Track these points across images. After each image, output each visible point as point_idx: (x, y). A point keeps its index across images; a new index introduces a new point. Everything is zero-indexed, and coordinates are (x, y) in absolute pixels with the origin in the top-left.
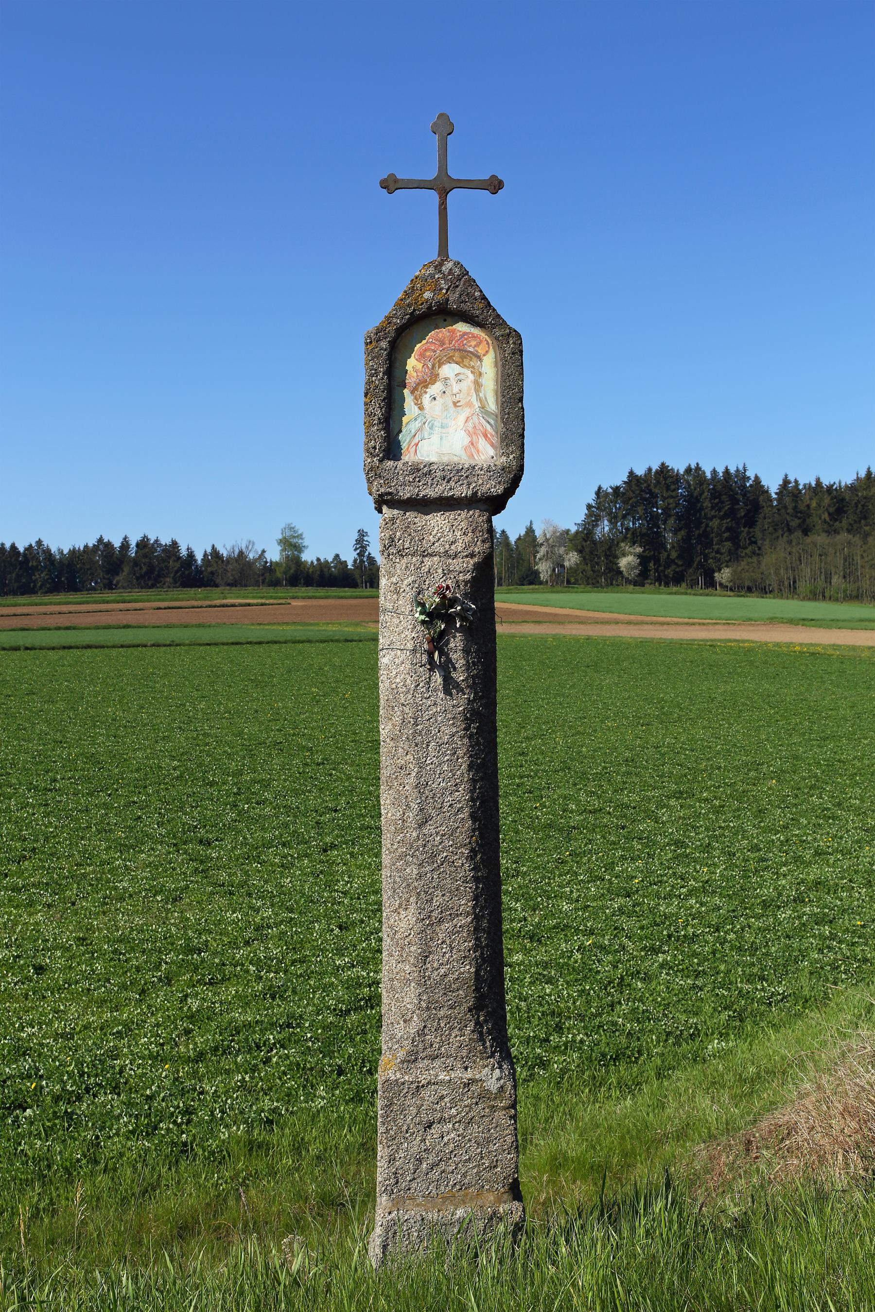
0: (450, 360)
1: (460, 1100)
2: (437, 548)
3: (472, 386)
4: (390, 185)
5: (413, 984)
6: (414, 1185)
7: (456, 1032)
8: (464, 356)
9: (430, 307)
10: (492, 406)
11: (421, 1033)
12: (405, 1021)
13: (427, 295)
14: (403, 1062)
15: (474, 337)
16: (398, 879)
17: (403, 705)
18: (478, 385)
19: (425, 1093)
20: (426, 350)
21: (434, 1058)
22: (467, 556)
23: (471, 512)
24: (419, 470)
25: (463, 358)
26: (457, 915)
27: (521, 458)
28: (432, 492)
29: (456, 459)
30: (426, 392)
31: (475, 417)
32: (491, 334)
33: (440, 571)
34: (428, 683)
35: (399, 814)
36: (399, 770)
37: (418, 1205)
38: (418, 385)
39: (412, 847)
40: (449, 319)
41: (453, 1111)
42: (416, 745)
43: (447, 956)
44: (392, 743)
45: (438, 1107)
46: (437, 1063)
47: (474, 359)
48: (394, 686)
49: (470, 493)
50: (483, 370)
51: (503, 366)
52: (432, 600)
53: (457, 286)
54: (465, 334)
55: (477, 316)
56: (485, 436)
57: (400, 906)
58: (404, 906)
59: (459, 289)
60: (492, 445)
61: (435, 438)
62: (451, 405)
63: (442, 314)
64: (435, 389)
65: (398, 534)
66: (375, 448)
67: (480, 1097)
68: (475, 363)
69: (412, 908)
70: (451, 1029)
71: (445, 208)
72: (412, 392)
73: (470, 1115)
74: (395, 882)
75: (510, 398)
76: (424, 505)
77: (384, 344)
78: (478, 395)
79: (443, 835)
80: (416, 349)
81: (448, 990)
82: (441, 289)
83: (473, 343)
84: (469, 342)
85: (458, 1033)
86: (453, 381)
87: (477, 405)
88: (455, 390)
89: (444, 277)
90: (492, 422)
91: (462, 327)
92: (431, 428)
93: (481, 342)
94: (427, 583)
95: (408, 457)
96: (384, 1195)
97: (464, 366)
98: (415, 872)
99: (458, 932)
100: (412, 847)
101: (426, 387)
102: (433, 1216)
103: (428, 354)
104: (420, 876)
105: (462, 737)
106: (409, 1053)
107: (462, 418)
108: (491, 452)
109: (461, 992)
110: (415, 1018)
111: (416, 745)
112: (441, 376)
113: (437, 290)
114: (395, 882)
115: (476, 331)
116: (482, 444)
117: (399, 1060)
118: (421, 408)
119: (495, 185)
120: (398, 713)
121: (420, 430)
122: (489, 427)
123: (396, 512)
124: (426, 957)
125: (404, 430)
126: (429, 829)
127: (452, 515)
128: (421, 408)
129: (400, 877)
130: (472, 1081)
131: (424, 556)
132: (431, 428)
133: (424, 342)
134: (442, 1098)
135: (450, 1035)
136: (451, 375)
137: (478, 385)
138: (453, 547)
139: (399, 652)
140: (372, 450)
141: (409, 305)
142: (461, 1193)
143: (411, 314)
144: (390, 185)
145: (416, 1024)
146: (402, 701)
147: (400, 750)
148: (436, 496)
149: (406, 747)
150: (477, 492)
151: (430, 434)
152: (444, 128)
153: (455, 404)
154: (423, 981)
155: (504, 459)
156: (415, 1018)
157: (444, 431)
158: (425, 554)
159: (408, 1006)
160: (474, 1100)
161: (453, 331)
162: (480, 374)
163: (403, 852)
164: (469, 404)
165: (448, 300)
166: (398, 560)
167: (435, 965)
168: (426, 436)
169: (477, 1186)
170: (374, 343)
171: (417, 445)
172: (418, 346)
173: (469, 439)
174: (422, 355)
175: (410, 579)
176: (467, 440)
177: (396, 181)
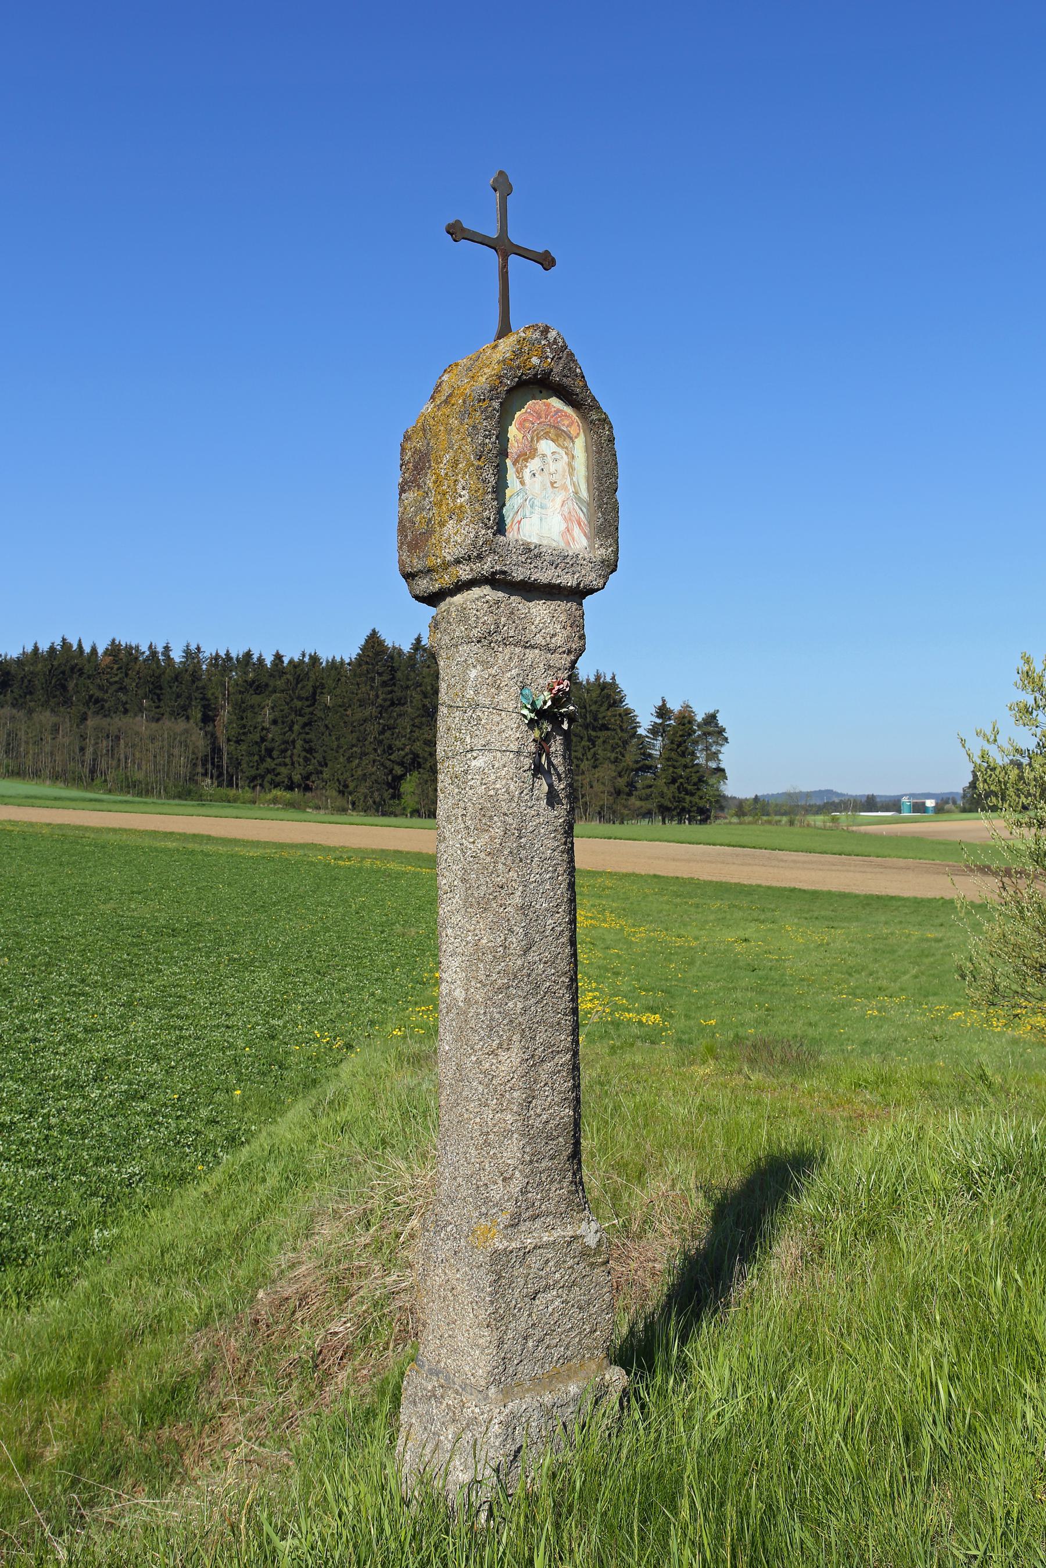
0: (546, 436)
1: (564, 1262)
2: (539, 639)
3: (567, 468)
4: (456, 232)
5: (515, 1136)
6: (520, 1368)
7: (556, 1185)
8: (560, 435)
9: (536, 375)
10: (584, 494)
11: (524, 1192)
12: (504, 1180)
13: (535, 360)
14: (506, 1227)
15: (567, 416)
16: (497, 1016)
17: (505, 814)
18: (571, 467)
19: (531, 1259)
20: (525, 420)
21: (534, 1218)
22: (564, 652)
23: (569, 604)
24: (530, 550)
25: (558, 436)
26: (558, 1052)
27: (616, 552)
28: (544, 576)
29: (554, 544)
30: (526, 467)
31: (570, 502)
32: (584, 417)
33: (541, 665)
34: (532, 790)
35: (499, 940)
36: (498, 889)
37: (528, 1390)
38: (519, 456)
39: (516, 977)
40: (544, 392)
41: (557, 1275)
42: (521, 861)
43: (549, 1099)
44: (488, 859)
45: (543, 1273)
46: (538, 1224)
47: (568, 440)
48: (492, 793)
49: (575, 583)
50: (575, 453)
51: (599, 452)
52: (544, 699)
53: (560, 358)
54: (558, 411)
55: (577, 395)
56: (580, 525)
57: (500, 1046)
58: (505, 1046)
59: (562, 361)
60: (585, 535)
61: (535, 518)
62: (549, 484)
63: (540, 384)
64: (534, 464)
65: (503, 619)
66: (489, 519)
67: (583, 1254)
68: (567, 443)
69: (516, 1047)
70: (552, 1182)
71: (507, 272)
72: (514, 464)
73: (573, 1276)
74: (492, 1019)
75: (608, 487)
76: (530, 590)
77: (496, 404)
78: (572, 479)
79: (546, 963)
80: (516, 416)
81: (550, 1138)
82: (547, 357)
83: (566, 422)
84: (562, 420)
85: (558, 1186)
86: (549, 459)
87: (571, 489)
88: (552, 470)
89: (549, 345)
90: (585, 510)
91: (555, 403)
92: (532, 507)
93: (572, 423)
94: (530, 677)
95: (512, 534)
96: (492, 1387)
97: (559, 445)
98: (520, 1005)
99: (559, 1072)
100: (516, 977)
101: (526, 460)
102: (548, 1399)
103: (527, 424)
104: (525, 1010)
105: (562, 852)
106: (513, 1216)
107: (558, 501)
108: (584, 542)
109: (561, 1139)
110: (517, 1174)
111: (521, 861)
112: (540, 451)
113: (543, 358)
114: (492, 1019)
115: (569, 410)
116: (577, 531)
117: (502, 1226)
118: (522, 483)
119: (546, 261)
120: (499, 824)
121: (522, 506)
122: (582, 515)
123: (500, 594)
124: (530, 1102)
125: (508, 504)
126: (532, 956)
127: (553, 605)
128: (522, 483)
129: (500, 1013)
130: (575, 1238)
131: (526, 647)
132: (532, 507)
133: (523, 410)
134: (547, 1262)
135: (550, 1189)
136: (548, 453)
137: (571, 467)
138: (553, 641)
139: (499, 754)
140: (486, 521)
141: (519, 367)
142: (565, 1367)
143: (520, 378)
144: (456, 232)
145: (518, 1182)
146: (505, 810)
147: (500, 866)
148: (546, 581)
149: (509, 862)
150: (579, 584)
151: (532, 513)
152: (503, 186)
153: (552, 484)
154: (527, 1133)
155: (603, 551)
156: (517, 1174)
157: (543, 511)
158: (528, 646)
159: (509, 1161)
160: (576, 1260)
161: (548, 405)
162: (573, 457)
163: (504, 984)
164: (564, 487)
165: (552, 370)
166: (500, 649)
167: (538, 1111)
168: (528, 514)
169: (579, 1357)
170: (487, 402)
171: (519, 522)
172: (518, 413)
173: (565, 526)
174: (521, 427)
175: (514, 672)
176: (563, 526)
177: (463, 230)
